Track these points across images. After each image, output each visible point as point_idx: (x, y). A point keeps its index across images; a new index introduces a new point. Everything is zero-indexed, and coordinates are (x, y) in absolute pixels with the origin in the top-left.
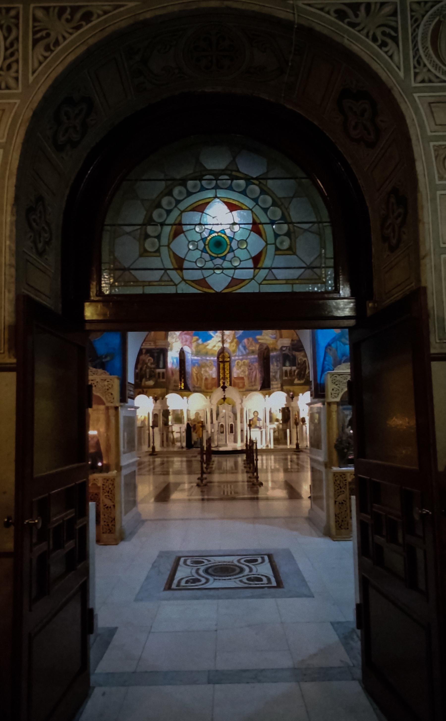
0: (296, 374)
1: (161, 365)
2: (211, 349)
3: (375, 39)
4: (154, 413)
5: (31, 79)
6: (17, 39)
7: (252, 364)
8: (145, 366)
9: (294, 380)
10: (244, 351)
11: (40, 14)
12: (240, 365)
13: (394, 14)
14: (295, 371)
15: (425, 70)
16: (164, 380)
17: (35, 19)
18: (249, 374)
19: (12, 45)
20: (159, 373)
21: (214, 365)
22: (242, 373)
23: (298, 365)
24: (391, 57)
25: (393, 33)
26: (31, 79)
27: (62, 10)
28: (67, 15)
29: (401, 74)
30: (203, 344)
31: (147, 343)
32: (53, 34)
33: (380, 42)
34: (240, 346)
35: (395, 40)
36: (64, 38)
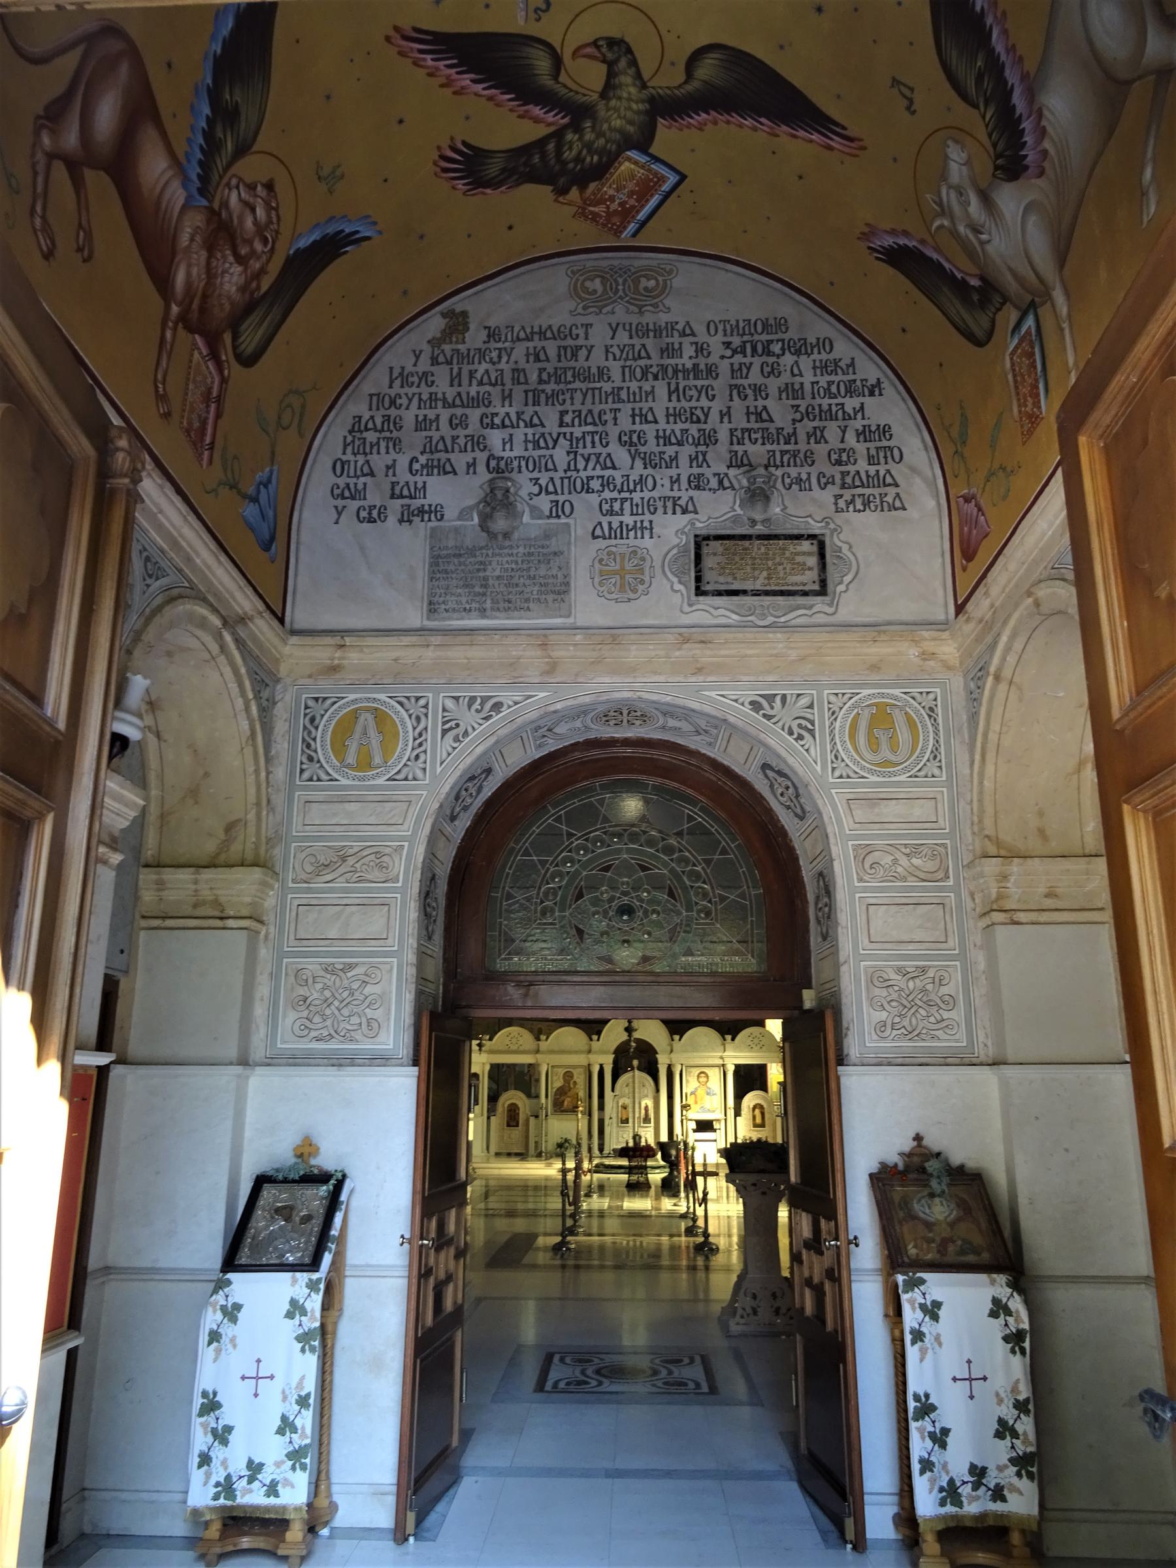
3: (791, 733)
5: (439, 770)
6: (426, 729)
11: (450, 704)
13: (811, 706)
15: (843, 764)
17: (444, 710)
19: (420, 735)
24: (807, 750)
25: (810, 727)
26: (439, 770)
27: (472, 700)
28: (476, 706)
29: (818, 768)
32: (461, 724)
33: (795, 736)
35: (811, 732)
36: (474, 729)
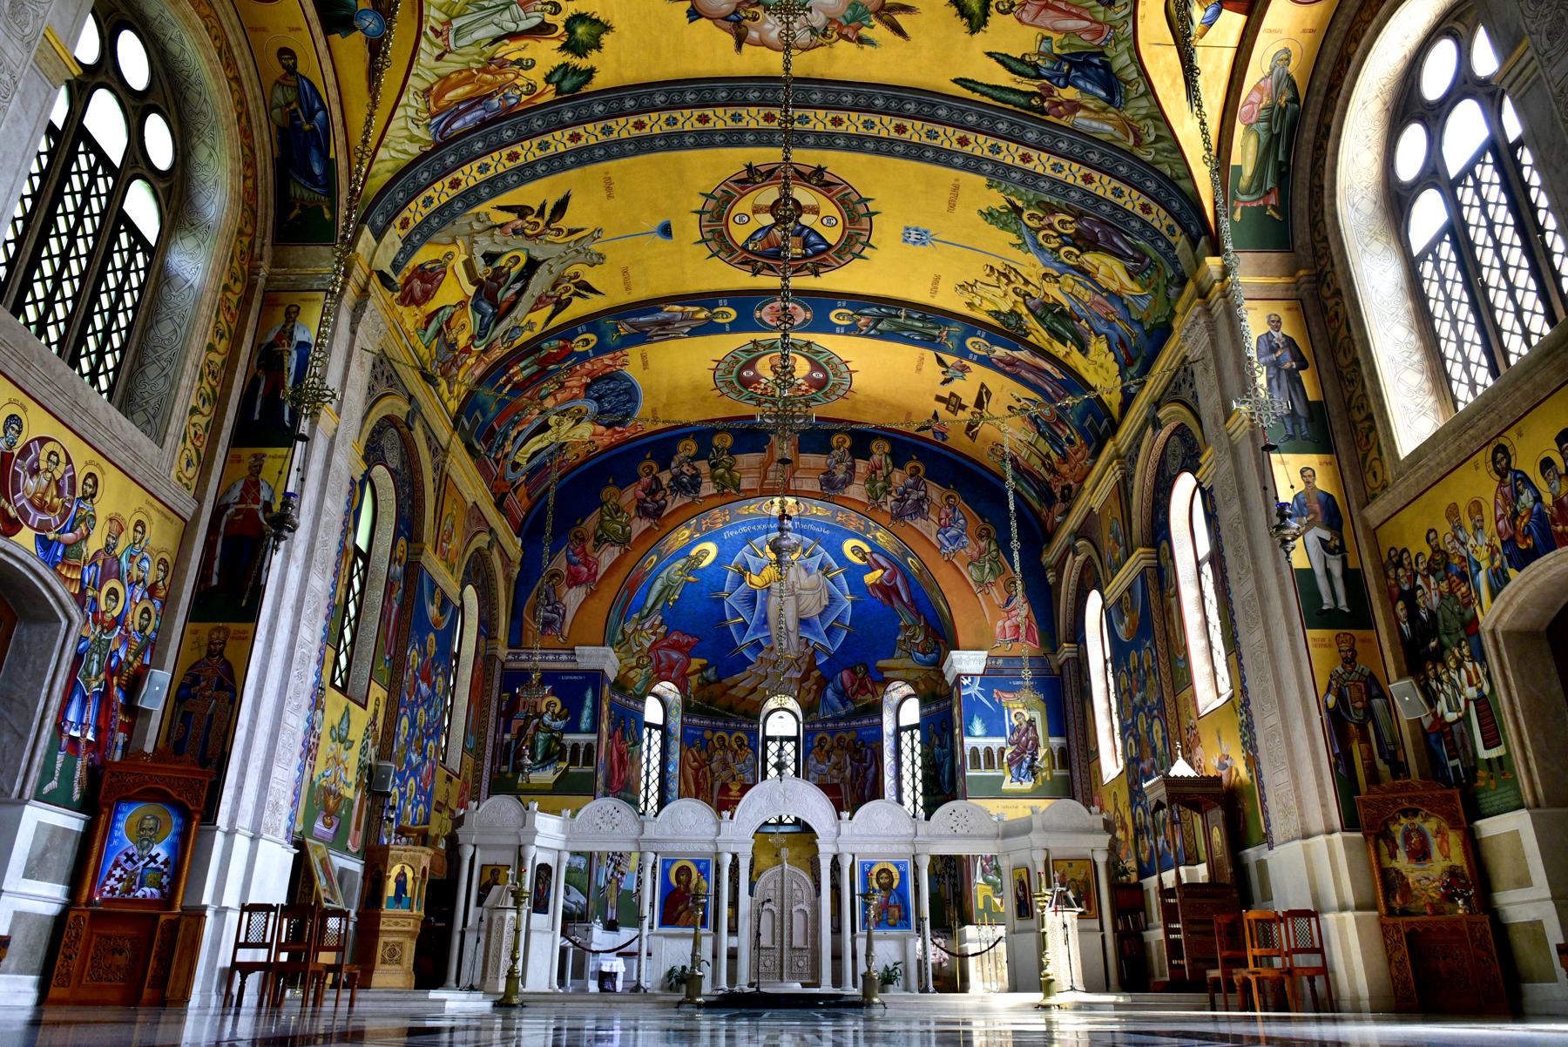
0: (1005, 760)
1: (585, 723)
2: (744, 699)
4: (537, 863)
7: (863, 744)
8: (536, 721)
9: (1002, 778)
10: (840, 706)
12: (827, 747)
14: (1002, 751)
16: (589, 769)
18: (856, 773)
20: (575, 747)
21: (749, 746)
22: (835, 772)
23: (1012, 734)
30: (719, 680)
31: (546, 655)
34: (829, 693)
